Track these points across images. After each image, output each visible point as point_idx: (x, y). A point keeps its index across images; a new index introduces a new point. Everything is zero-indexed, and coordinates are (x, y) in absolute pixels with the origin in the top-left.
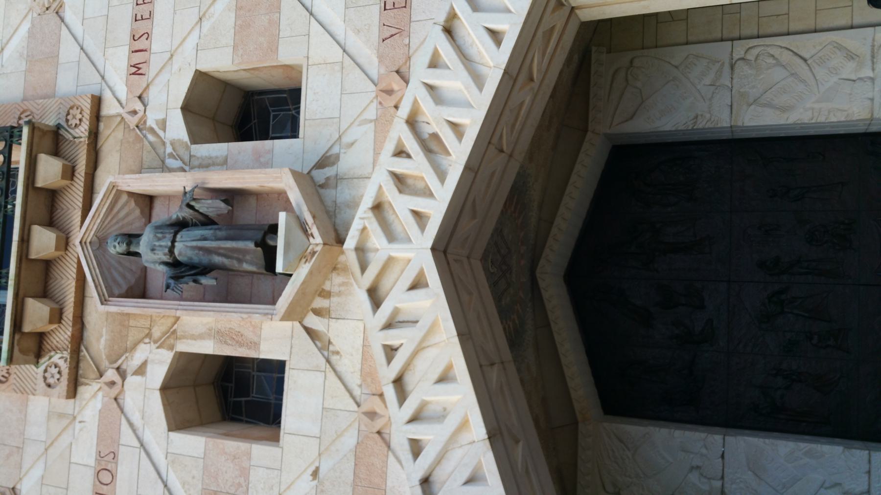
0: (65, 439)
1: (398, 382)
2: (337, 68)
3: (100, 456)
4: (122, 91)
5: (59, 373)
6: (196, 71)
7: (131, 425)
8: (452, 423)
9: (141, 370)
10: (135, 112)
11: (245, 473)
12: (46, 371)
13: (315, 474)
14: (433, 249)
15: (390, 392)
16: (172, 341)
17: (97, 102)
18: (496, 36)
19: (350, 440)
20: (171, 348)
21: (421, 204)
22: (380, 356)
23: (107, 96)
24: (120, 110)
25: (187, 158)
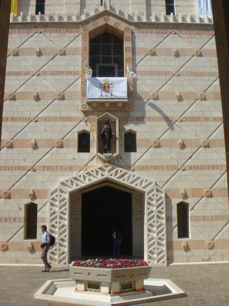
0: (74, 109)
1: (88, 173)
2: (135, 159)
3: (72, 118)
4: (133, 116)
5: (85, 108)
6: (136, 132)
7: (78, 124)
8: (84, 181)
9: (87, 125)
10: (130, 119)
11: (73, 147)
12: (85, 105)
13: (74, 159)
14: (107, 177)
15: (87, 172)
16: (92, 131)
17: (133, 111)
18: (137, 185)
19: (79, 164)
20: (91, 131)
21: (113, 175)
22: (92, 169)
23: (134, 112)
24: (131, 115)
25: (122, 131)
